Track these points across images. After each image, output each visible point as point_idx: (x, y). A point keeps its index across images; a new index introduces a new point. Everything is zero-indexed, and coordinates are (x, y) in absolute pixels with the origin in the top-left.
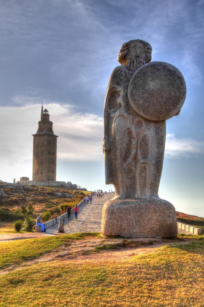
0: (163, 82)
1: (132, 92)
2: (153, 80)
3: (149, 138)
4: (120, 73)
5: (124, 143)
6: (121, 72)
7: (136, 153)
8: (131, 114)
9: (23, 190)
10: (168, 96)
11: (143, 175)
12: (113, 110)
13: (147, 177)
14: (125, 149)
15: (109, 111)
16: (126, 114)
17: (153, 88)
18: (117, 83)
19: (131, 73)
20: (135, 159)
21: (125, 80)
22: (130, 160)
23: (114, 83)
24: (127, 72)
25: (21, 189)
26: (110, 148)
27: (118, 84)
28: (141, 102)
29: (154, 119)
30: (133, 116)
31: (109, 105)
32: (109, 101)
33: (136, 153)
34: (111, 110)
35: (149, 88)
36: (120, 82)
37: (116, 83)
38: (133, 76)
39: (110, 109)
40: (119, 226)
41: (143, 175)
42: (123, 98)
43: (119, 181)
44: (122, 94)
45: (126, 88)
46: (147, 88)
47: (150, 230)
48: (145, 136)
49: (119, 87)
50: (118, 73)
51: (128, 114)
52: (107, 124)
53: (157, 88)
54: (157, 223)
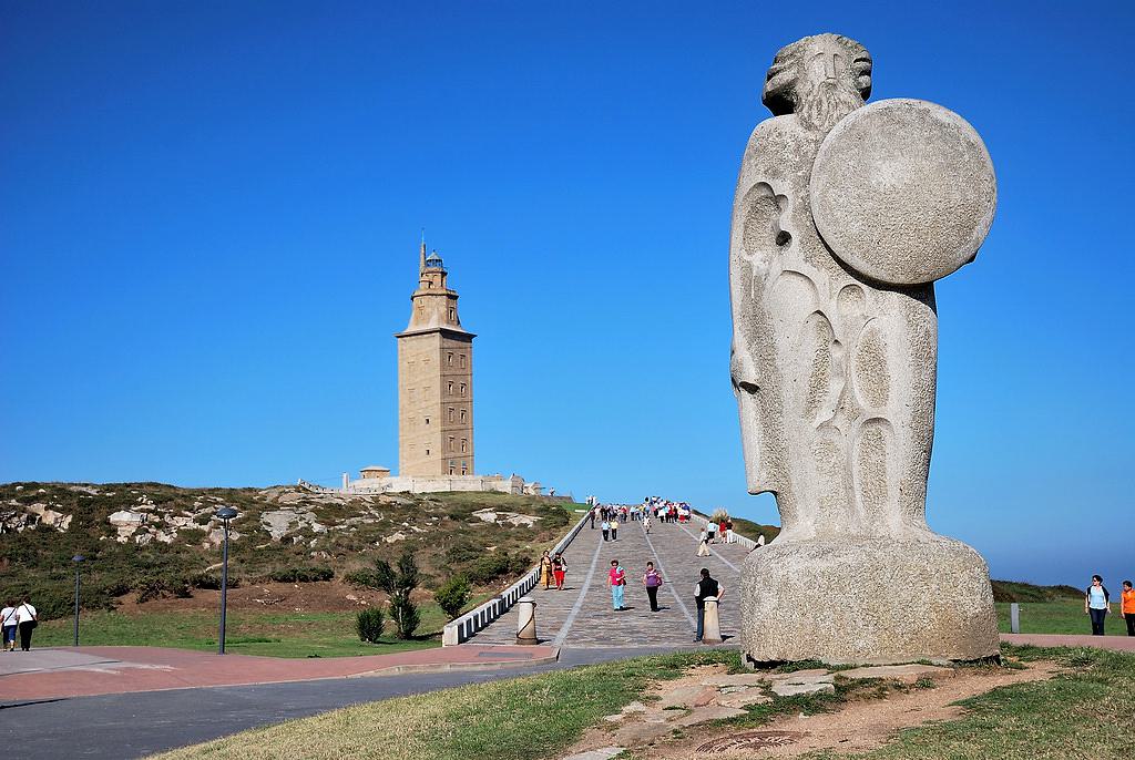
1: (824, 194)
2: (891, 156)
3: (888, 341)
9: (374, 508)
10: (941, 206)
11: (874, 458)
17: (893, 181)
22: (824, 414)
24: (802, 135)
25: (368, 505)
27: (776, 174)
29: (901, 279)
35: (879, 184)
36: (781, 168)
38: (823, 147)
39: (750, 253)
40: (809, 629)
48: (873, 333)
49: (778, 181)
54: (933, 615)
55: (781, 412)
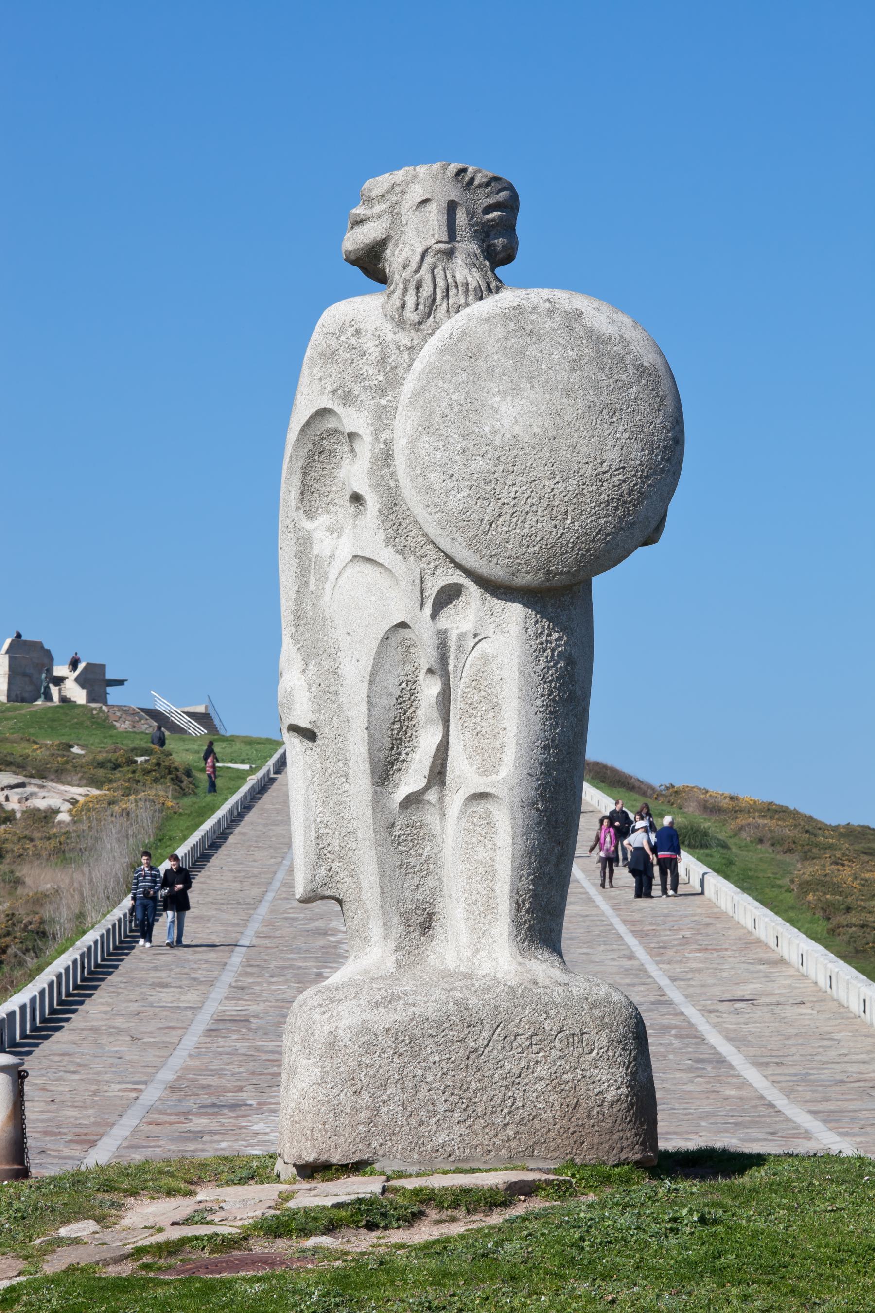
0: (564, 400)
3: (505, 674)
4: (353, 340)
5: (384, 697)
6: (358, 332)
7: (443, 749)
8: (413, 552)
12: (323, 519)
13: (497, 866)
14: (386, 725)
15: (308, 525)
16: (387, 555)
17: (517, 430)
18: (340, 392)
19: (406, 342)
20: (440, 773)
21: (381, 378)
23: (329, 388)
24: (390, 336)
26: (314, 718)
27: (347, 399)
28: (457, 500)
30: (422, 566)
31: (302, 494)
32: (305, 475)
33: (443, 749)
34: (316, 523)
35: (494, 433)
36: (357, 389)
37: (334, 392)
41: (482, 854)
42: (372, 473)
43: (365, 884)
44: (365, 449)
45: (383, 418)
46: (487, 429)
47: (517, 1133)
48: (485, 660)
50: (343, 338)
51: (398, 552)
52: (297, 592)
53: (536, 430)
55: (346, 776)
